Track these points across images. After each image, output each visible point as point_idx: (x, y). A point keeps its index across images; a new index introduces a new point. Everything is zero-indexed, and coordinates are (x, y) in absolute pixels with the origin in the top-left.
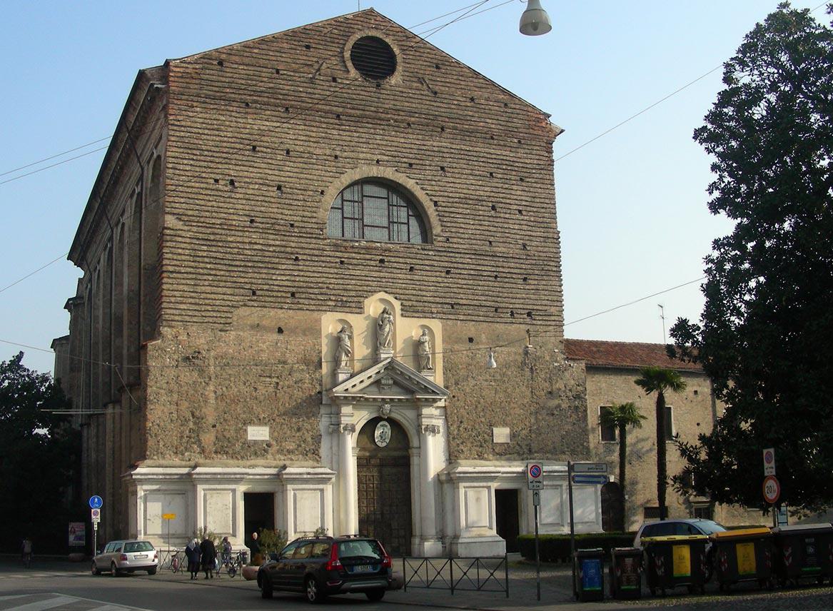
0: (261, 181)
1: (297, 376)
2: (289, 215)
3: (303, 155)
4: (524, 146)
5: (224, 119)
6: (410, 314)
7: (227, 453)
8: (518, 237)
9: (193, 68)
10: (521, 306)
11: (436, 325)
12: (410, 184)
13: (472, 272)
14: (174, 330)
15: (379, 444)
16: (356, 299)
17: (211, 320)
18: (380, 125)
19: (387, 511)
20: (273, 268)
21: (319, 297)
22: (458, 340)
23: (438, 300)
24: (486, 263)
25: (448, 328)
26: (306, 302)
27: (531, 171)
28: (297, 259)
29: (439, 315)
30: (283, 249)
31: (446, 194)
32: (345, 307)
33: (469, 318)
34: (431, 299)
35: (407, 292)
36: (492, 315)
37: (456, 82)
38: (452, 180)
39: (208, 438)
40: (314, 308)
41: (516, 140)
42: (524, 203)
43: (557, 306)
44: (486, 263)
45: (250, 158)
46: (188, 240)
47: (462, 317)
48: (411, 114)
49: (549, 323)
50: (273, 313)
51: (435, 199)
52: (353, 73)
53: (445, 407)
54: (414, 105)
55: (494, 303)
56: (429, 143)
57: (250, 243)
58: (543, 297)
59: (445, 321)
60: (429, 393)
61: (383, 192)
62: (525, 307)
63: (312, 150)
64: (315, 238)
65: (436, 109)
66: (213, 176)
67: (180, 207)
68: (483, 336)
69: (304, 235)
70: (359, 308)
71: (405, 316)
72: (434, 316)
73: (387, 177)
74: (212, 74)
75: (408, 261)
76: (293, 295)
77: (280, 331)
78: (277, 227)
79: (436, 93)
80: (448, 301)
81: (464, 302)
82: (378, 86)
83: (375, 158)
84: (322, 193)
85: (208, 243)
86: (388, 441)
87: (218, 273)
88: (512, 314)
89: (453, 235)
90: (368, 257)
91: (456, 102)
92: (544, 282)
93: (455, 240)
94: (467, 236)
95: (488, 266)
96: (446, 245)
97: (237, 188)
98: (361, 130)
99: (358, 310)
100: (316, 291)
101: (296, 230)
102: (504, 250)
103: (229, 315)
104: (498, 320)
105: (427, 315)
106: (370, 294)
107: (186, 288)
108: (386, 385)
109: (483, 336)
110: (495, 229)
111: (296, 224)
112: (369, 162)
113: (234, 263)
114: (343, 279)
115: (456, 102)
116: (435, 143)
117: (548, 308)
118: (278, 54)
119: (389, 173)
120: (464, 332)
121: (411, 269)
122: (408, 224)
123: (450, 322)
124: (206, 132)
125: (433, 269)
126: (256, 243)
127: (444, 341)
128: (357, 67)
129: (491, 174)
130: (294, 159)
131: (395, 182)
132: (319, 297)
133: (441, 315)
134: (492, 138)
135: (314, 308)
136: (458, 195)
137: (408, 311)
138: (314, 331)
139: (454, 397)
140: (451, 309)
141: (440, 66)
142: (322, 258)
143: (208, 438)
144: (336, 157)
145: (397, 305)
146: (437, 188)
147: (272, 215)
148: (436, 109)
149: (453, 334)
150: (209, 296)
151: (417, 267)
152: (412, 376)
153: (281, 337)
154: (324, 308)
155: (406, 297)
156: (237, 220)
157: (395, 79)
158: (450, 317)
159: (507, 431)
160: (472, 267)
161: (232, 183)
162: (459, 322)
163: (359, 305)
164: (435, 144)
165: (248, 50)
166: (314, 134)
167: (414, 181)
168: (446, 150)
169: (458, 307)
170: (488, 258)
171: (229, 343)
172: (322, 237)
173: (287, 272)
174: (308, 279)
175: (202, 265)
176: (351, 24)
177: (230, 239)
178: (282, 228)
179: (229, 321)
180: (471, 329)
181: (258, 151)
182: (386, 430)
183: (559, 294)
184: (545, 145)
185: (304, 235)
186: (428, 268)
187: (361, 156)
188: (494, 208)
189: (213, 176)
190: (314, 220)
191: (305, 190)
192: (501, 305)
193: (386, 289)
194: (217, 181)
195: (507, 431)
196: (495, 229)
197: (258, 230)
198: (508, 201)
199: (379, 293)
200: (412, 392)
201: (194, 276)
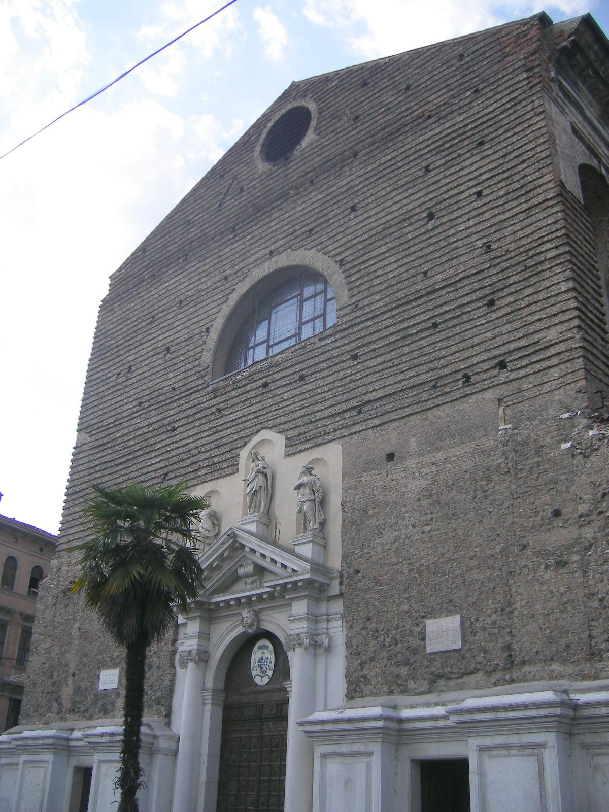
5: (133, 304)
10: (484, 357)
15: (258, 680)
23: (338, 409)
29: (338, 434)
30: (160, 424)
33: (387, 418)
34: (327, 413)
38: (366, 215)
49: (547, 363)
55: (431, 373)
58: (529, 319)
59: (347, 439)
64: (195, 392)
68: (413, 442)
73: (281, 266)
81: (379, 394)
83: (267, 251)
84: (207, 330)
86: (270, 673)
92: (530, 291)
93: (366, 301)
105: (320, 441)
106: (247, 440)
109: (413, 442)
112: (259, 262)
119: (283, 260)
121: (302, 378)
127: (344, 475)
134: (430, 117)
137: (293, 447)
158: (354, 430)
159: (452, 622)
160: (392, 329)
162: (370, 432)
167: (314, 249)
169: (366, 408)
180: (389, 438)
188: (431, 216)
193: (267, 424)
195: (452, 622)
199: (259, 434)
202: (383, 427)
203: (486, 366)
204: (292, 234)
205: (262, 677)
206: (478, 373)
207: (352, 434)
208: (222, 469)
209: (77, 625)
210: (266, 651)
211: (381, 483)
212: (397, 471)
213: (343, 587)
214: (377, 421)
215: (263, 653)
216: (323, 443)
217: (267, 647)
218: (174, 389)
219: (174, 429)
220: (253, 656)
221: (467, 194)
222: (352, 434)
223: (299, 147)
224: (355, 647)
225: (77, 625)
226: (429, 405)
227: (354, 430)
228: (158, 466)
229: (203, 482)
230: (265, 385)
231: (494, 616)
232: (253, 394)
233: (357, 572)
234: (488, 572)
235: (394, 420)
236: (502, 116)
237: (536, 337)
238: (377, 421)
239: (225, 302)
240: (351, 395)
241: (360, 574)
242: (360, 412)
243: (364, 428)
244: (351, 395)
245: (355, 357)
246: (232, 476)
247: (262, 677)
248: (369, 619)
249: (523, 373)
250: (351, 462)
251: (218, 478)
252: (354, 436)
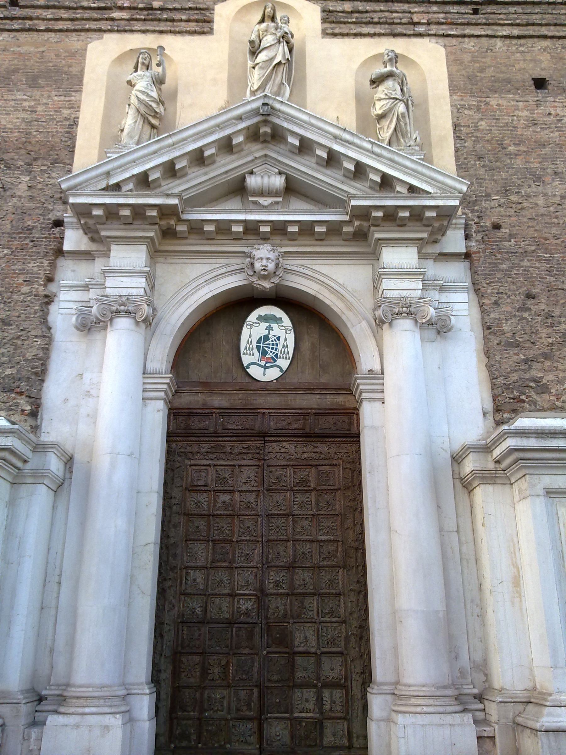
6: (344, 29)
15: (255, 372)
19: (277, 584)
25: (467, 58)
29: (434, 29)
32: (159, 20)
33: (531, 31)
47: (506, 31)
53: (467, 256)
59: (454, 41)
71: (334, 35)
72: (421, 29)
86: (284, 364)
99: (192, 26)
105: (399, 29)
108: (262, 193)
120: (517, 67)
123: (469, 44)
127: (453, 88)
149: (482, 70)
152: (336, 147)
158: (468, 31)
162: (499, 43)
182: (277, 331)
202: (522, 41)
205: (265, 367)
207: (464, 36)
208: (173, 20)
210: (275, 326)
211: (526, 113)
212: (556, 104)
213: (473, 244)
214: (516, 31)
215: (269, 328)
216: (405, 35)
217: (278, 320)
220: (245, 331)
222: (464, 36)
224: (509, 335)
229: (125, 31)
233: (497, 227)
235: (545, 37)
238: (516, 31)
241: (505, 231)
242: (476, 12)
243: (489, 33)
246: (196, 38)
247: (265, 367)
248: (530, 296)
250: (464, 72)
251: (162, 32)
252: (466, 40)
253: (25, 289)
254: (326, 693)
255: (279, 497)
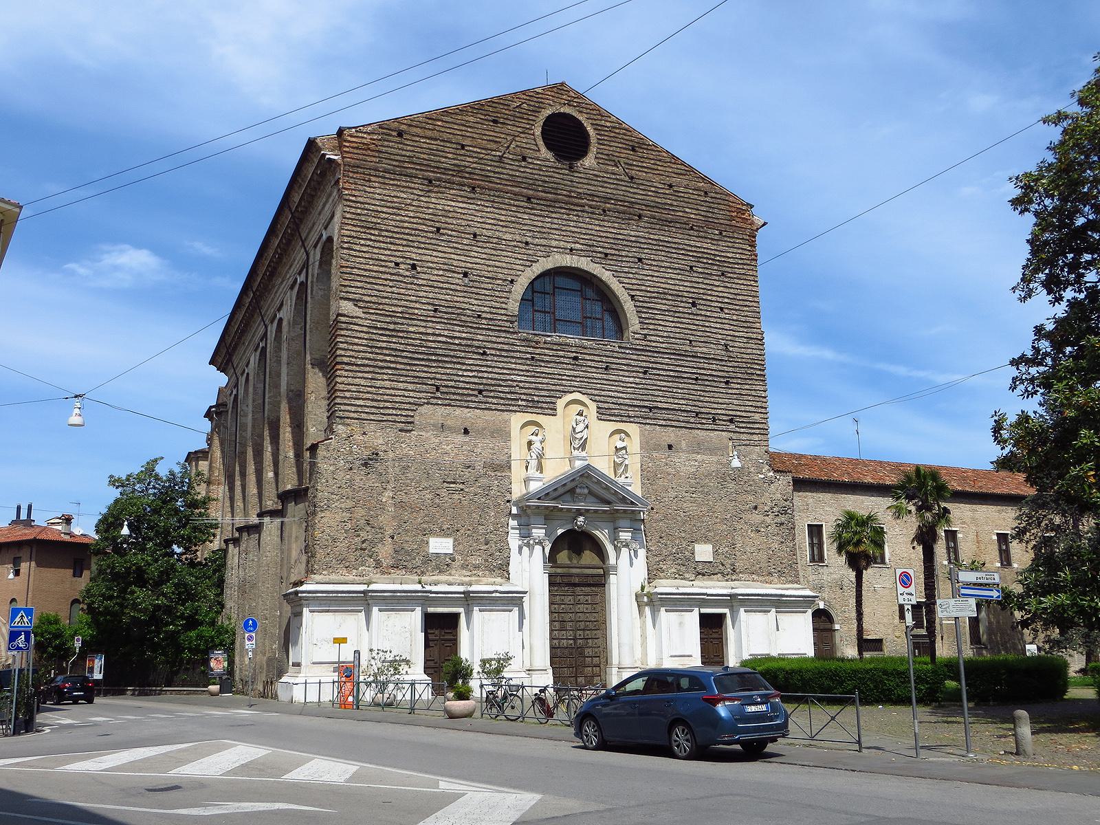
0: (445, 267)
1: (483, 481)
2: (474, 305)
3: (491, 240)
4: (726, 239)
5: (405, 196)
7: (405, 567)
8: (720, 337)
9: (371, 139)
10: (723, 412)
11: (633, 429)
12: (606, 276)
13: (672, 374)
14: (350, 428)
16: (548, 400)
17: (390, 418)
18: (574, 210)
19: (580, 635)
20: (459, 363)
21: (509, 396)
22: (657, 448)
23: (636, 403)
24: (687, 364)
26: (494, 401)
27: (733, 265)
28: (484, 353)
29: (637, 420)
30: (469, 342)
31: (643, 288)
35: (603, 393)
36: (692, 420)
37: (653, 166)
38: (650, 273)
39: (385, 551)
40: (503, 408)
41: (717, 232)
42: (726, 300)
43: (761, 413)
44: (687, 364)
45: (433, 241)
46: (365, 329)
48: (607, 199)
49: (753, 431)
50: (458, 411)
51: (633, 293)
52: (545, 153)
54: (609, 191)
56: (626, 232)
57: (434, 334)
60: (628, 504)
61: (576, 285)
62: (727, 412)
63: (501, 234)
64: (505, 331)
65: (632, 195)
66: (393, 259)
67: (356, 293)
68: (684, 444)
69: (492, 328)
70: (551, 409)
71: (601, 419)
74: (392, 146)
75: (604, 359)
76: (480, 392)
77: (466, 432)
78: (463, 318)
79: (632, 178)
80: (647, 404)
82: (571, 167)
83: (569, 246)
84: (512, 281)
85: (387, 333)
87: (399, 366)
88: (714, 420)
89: (652, 332)
90: (561, 353)
91: (653, 189)
93: (653, 338)
94: (666, 334)
95: (688, 366)
96: (645, 343)
97: (419, 273)
98: (554, 215)
100: (507, 389)
101: (484, 321)
102: (705, 350)
103: (411, 413)
104: (699, 426)
107: (362, 382)
109: (684, 444)
110: (695, 327)
111: (484, 315)
113: (416, 356)
114: (534, 377)
115: (653, 189)
116: (632, 231)
117: (753, 414)
118: (464, 128)
119: (584, 263)
121: (606, 369)
122: (602, 319)
124: (385, 210)
125: (630, 368)
126: (440, 335)
128: (549, 147)
129: (691, 267)
130: (480, 244)
131: (590, 273)
132: (509, 396)
133: (641, 421)
134: (692, 229)
135: (503, 408)
136: (656, 290)
138: (503, 434)
139: (652, 509)
140: (648, 413)
141: (637, 149)
142: (512, 354)
143: (385, 551)
144: (527, 243)
145: (593, 406)
146: (634, 281)
147: (458, 305)
148: (632, 195)
150: (388, 392)
151: (614, 366)
153: (467, 439)
154: (515, 408)
155: (602, 399)
156: (422, 309)
157: (589, 161)
158: (648, 421)
159: (708, 548)
161: (414, 267)
163: (551, 406)
164: (632, 233)
165: (430, 122)
166: (503, 218)
168: (643, 241)
169: (656, 411)
170: (689, 359)
171: (408, 446)
172: (511, 330)
173: (474, 368)
174: (496, 376)
175: (380, 357)
176: (542, 98)
177: (411, 329)
178: (468, 319)
179: (410, 420)
180: (670, 435)
181: (444, 234)
183: (764, 400)
184: (747, 238)
185: (492, 328)
186: (625, 368)
187: (554, 243)
189: (393, 259)
190: (503, 312)
191: (493, 278)
192: (703, 410)
194: (397, 264)
195: (708, 548)
196: (695, 327)
197: (443, 320)
198: (709, 298)
200: (609, 503)
201: (371, 369)
203: (725, 418)
204: (590, 246)
206: (720, 420)
209: (389, 494)
218: (479, 316)
219: (484, 353)
221: (716, 304)
223: (581, 161)
225: (389, 494)
226: (693, 426)
227: (648, 421)
228: (472, 380)
230: (576, 358)
231: (727, 549)
232: (566, 361)
233: (652, 509)
234: (725, 526)
236: (736, 266)
237: (749, 414)
238: (664, 423)
239: (530, 267)
240: (644, 397)
244: (644, 397)
245: (645, 373)
249: (742, 430)
251: (538, 413)
253: (501, 530)
254: (594, 668)
255: (579, 606)
